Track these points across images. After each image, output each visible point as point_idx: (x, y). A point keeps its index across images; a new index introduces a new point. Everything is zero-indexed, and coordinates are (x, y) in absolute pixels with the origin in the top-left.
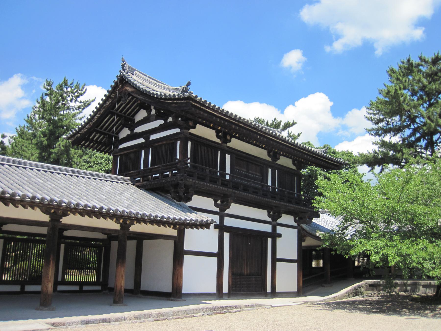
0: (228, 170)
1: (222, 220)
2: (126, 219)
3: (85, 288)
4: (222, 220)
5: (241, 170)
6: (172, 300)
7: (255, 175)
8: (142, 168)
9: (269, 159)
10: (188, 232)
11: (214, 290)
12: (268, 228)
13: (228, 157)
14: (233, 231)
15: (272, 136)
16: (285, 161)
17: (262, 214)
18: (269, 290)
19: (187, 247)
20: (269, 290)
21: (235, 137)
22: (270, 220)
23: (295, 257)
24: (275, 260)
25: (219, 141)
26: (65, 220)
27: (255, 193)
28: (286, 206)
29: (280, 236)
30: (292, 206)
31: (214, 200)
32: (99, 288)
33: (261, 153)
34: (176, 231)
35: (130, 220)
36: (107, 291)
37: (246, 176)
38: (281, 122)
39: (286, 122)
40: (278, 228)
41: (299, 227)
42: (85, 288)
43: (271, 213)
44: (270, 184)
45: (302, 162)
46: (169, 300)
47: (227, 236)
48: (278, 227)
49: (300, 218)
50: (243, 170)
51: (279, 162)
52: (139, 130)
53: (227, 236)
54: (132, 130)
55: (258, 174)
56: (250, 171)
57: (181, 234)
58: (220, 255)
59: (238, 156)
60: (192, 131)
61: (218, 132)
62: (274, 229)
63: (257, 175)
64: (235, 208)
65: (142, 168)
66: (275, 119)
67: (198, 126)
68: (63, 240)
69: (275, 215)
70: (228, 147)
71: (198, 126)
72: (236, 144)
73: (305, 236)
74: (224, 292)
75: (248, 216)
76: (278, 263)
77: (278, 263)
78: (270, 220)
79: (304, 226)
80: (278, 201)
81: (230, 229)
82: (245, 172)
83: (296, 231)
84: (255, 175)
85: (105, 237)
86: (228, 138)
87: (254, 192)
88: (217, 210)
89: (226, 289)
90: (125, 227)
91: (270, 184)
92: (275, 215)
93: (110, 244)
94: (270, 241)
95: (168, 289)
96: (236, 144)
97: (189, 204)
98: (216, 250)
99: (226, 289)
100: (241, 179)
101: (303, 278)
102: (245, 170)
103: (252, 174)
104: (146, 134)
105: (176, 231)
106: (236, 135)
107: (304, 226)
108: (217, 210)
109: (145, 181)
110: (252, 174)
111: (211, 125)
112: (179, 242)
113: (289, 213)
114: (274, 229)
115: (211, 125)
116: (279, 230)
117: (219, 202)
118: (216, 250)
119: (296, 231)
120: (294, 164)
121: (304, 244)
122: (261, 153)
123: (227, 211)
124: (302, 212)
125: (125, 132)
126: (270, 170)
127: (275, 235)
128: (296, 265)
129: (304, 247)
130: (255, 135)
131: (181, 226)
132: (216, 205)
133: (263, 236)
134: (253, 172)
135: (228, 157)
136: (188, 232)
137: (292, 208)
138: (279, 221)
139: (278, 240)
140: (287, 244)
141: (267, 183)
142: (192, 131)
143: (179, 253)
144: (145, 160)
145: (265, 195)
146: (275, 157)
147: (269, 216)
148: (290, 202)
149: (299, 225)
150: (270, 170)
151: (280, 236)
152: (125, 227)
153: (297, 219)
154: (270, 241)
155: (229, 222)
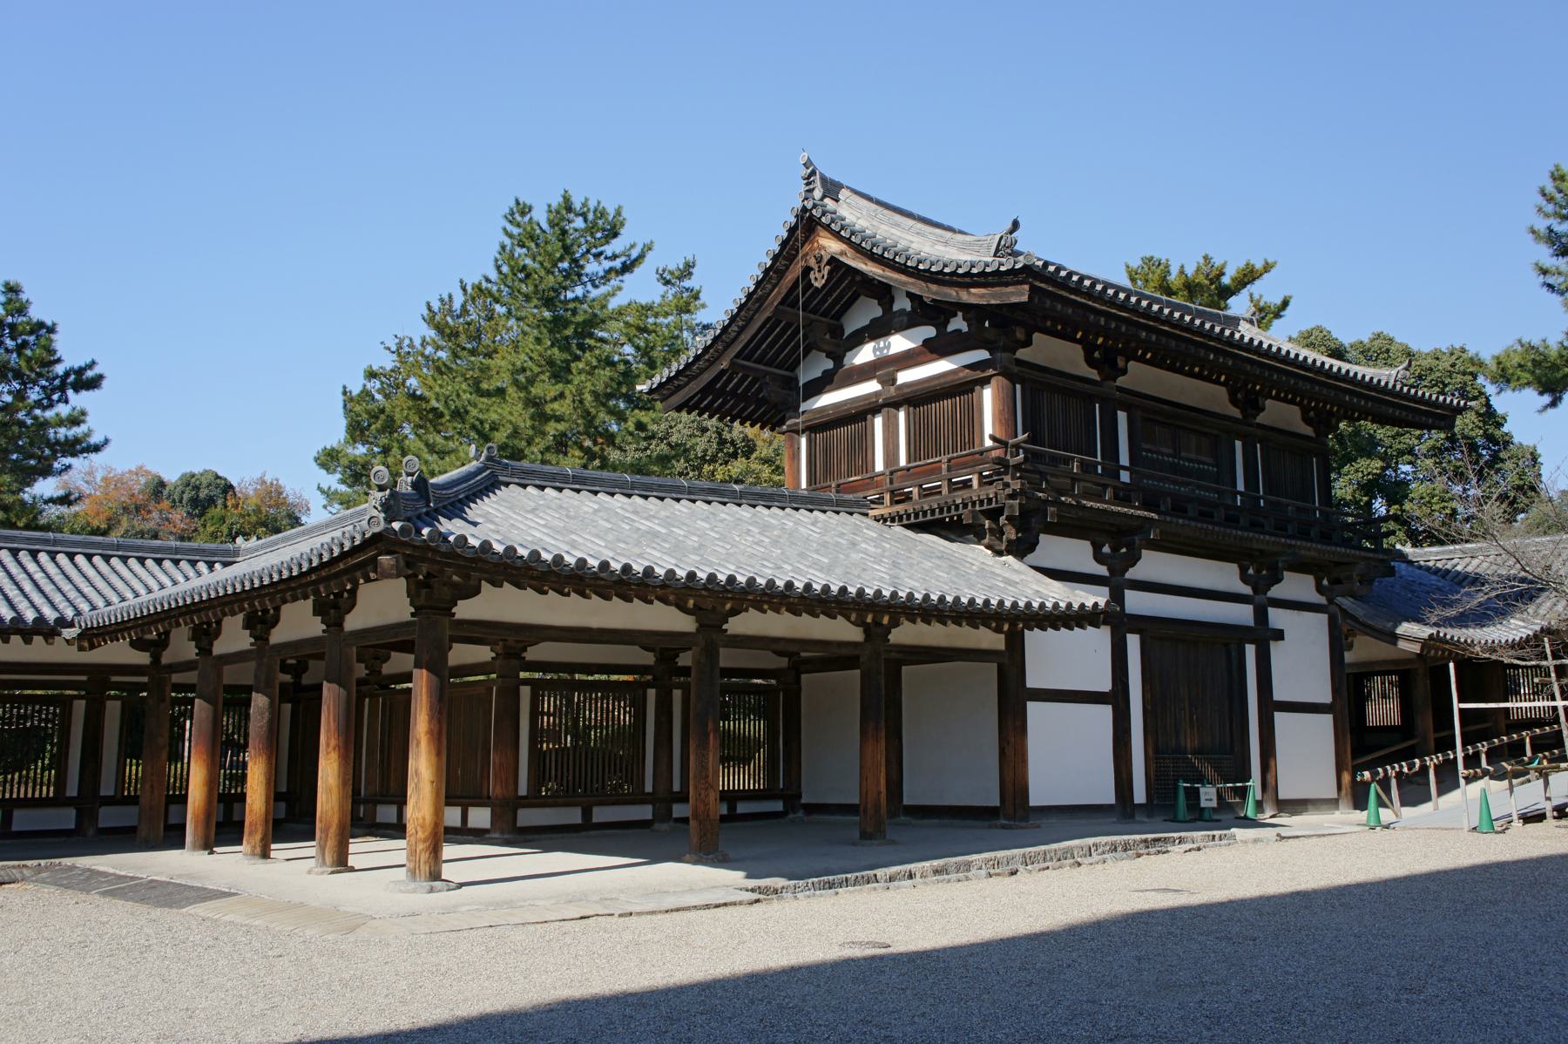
0: (1124, 460)
2: (876, 613)
3: (742, 808)
4: (1117, 597)
5: (1158, 453)
6: (1003, 827)
7: (1199, 462)
8: (879, 466)
9: (1235, 412)
10: (1035, 640)
11: (1108, 796)
12: (1243, 614)
13: (1122, 417)
14: (1145, 625)
15: (1248, 351)
16: (1280, 414)
17: (1225, 576)
21: (1142, 360)
22: (1247, 590)
23: (1326, 697)
24: (1269, 706)
25: (1094, 374)
26: (736, 625)
27: (1205, 516)
28: (1290, 546)
29: (1279, 635)
30: (1311, 550)
31: (1093, 544)
32: (779, 806)
33: (1211, 396)
34: (1002, 636)
35: (874, 612)
36: (800, 814)
37: (1175, 469)
38: (1224, 266)
39: (1242, 265)
40: (1273, 613)
41: (1333, 608)
42: (742, 808)
44: (1241, 486)
45: (1331, 413)
46: (996, 827)
47: (1133, 642)
48: (1271, 610)
49: (1335, 581)
51: (1261, 419)
52: (865, 354)
53: (1133, 642)
54: (838, 359)
57: (1016, 645)
58: (1117, 698)
59: (1154, 416)
60: (1022, 354)
61: (1089, 350)
62: (1261, 615)
65: (879, 466)
66: (1206, 258)
67: (1037, 337)
68: (676, 680)
69: (1262, 574)
70: (1120, 389)
71: (1037, 337)
72: (1140, 376)
73: (1351, 633)
74: (1137, 801)
75: (1187, 584)
76: (1278, 716)
77: (1278, 716)
78: (1247, 590)
79: (1346, 602)
80: (1271, 534)
81: (1141, 624)
82: (1168, 455)
83: (1324, 618)
84: (1199, 462)
85: (783, 662)
86: (1121, 362)
87: (1202, 514)
88: (1103, 570)
89: (1140, 796)
90: (876, 633)
91: (1241, 486)
92: (1262, 574)
93: (798, 681)
94: (1250, 651)
96: (1140, 376)
97: (1030, 558)
98: (1105, 684)
99: (1140, 796)
100: (1161, 479)
101: (1353, 758)
103: (1190, 460)
104: (884, 368)
105: (1002, 636)
106: (1144, 354)
107: (1346, 602)
108: (1103, 570)
109: (898, 502)
110: (1190, 460)
111: (1079, 335)
112: (1011, 663)
113: (1300, 567)
114: (1261, 615)
115: (1079, 335)
116: (1277, 617)
117: (1106, 549)
118: (1105, 684)
119: (1324, 618)
120: (1307, 420)
121: (1349, 657)
122: (1211, 396)
124: (1338, 564)
125: (818, 366)
127: (1265, 636)
128: (1327, 719)
129: (1352, 665)
130: (1202, 352)
131: (1017, 622)
132: (1099, 557)
133: (1232, 636)
134: (1193, 456)
135: (1122, 417)
136: (1035, 640)
137: (1312, 553)
138: (1276, 592)
139: (1276, 649)
140: (1301, 660)
141: (1235, 485)
142: (1022, 354)
143: (1014, 697)
144: (890, 444)
145: (1231, 520)
146: (1251, 405)
147: (1245, 578)
148: (1304, 534)
149: (1330, 601)
151: (1279, 635)
152: (876, 633)
153: (1325, 582)
154: (1250, 651)
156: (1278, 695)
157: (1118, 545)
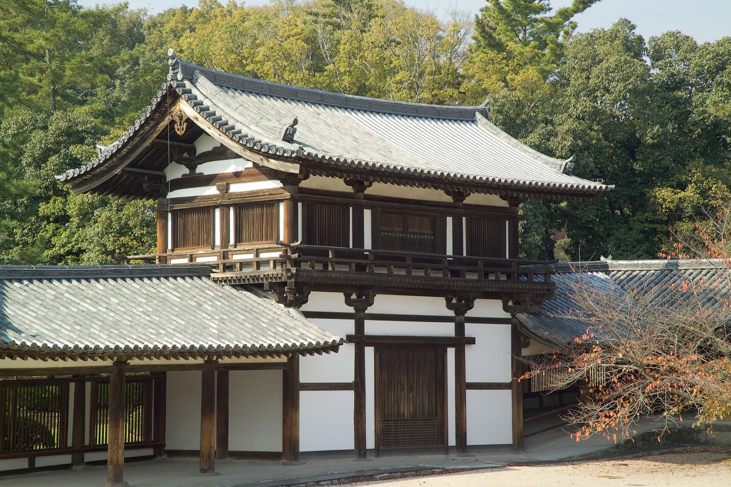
1: (360, 327)
4: (360, 327)
11: (350, 445)
12: (447, 330)
13: (367, 214)
17: (437, 306)
18: (452, 441)
19: (303, 379)
20: (452, 441)
29: (472, 341)
43: (454, 301)
49: (517, 303)
50: (396, 229)
53: (369, 353)
55: (424, 231)
56: (410, 230)
58: (358, 386)
62: (460, 329)
63: (423, 234)
64: (383, 303)
69: (461, 301)
77: (470, 393)
79: (522, 317)
84: (421, 234)
88: (351, 310)
92: (461, 301)
94: (451, 353)
95: (277, 446)
99: (370, 444)
102: (400, 229)
103: (414, 234)
107: (522, 317)
108: (351, 310)
110: (414, 234)
114: (460, 329)
116: (470, 330)
119: (508, 328)
123: (370, 310)
126: (449, 220)
127: (461, 342)
133: (438, 345)
139: (469, 350)
150: (449, 220)
151: (472, 341)
153: (510, 303)
154: (451, 353)
155: (372, 328)
156: (469, 379)
157: (360, 294)
